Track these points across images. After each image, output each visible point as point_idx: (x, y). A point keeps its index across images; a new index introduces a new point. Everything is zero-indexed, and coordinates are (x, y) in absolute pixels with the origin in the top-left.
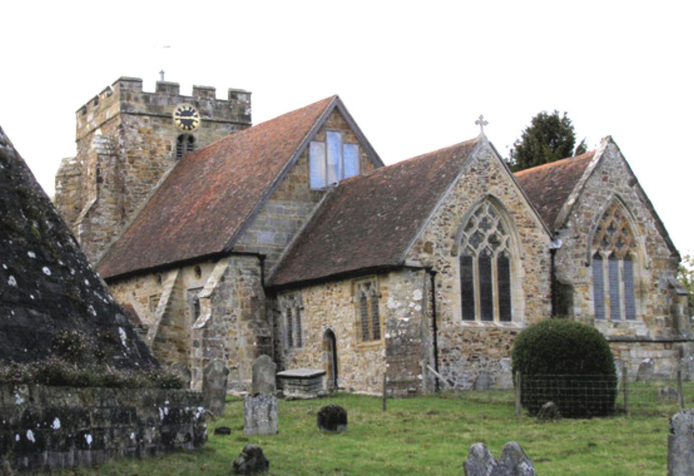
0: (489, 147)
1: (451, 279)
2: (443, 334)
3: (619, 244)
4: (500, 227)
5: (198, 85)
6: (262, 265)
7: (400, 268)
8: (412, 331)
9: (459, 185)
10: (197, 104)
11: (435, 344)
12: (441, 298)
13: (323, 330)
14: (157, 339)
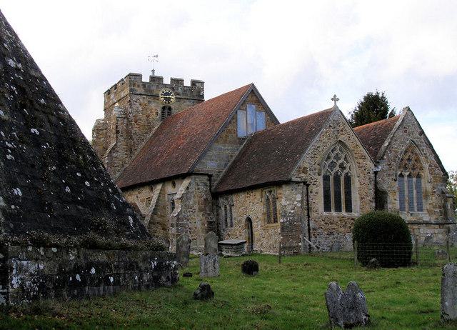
0: (340, 113)
3: (414, 169)
4: (345, 159)
5: (174, 77)
6: (210, 180)
7: (289, 182)
8: (296, 218)
11: (309, 225)
14: (150, 223)
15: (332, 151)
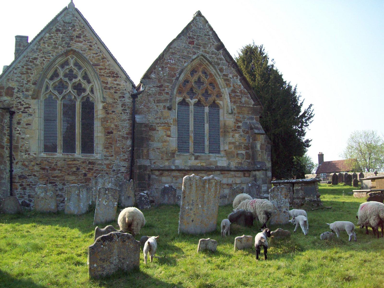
1: (30, 118)
2: (20, 163)
9: (42, 41)
11: (11, 171)
12: (19, 134)
15: (62, 66)
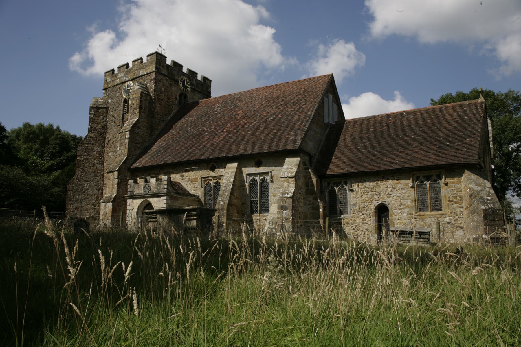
10: (189, 78)
13: (375, 204)
